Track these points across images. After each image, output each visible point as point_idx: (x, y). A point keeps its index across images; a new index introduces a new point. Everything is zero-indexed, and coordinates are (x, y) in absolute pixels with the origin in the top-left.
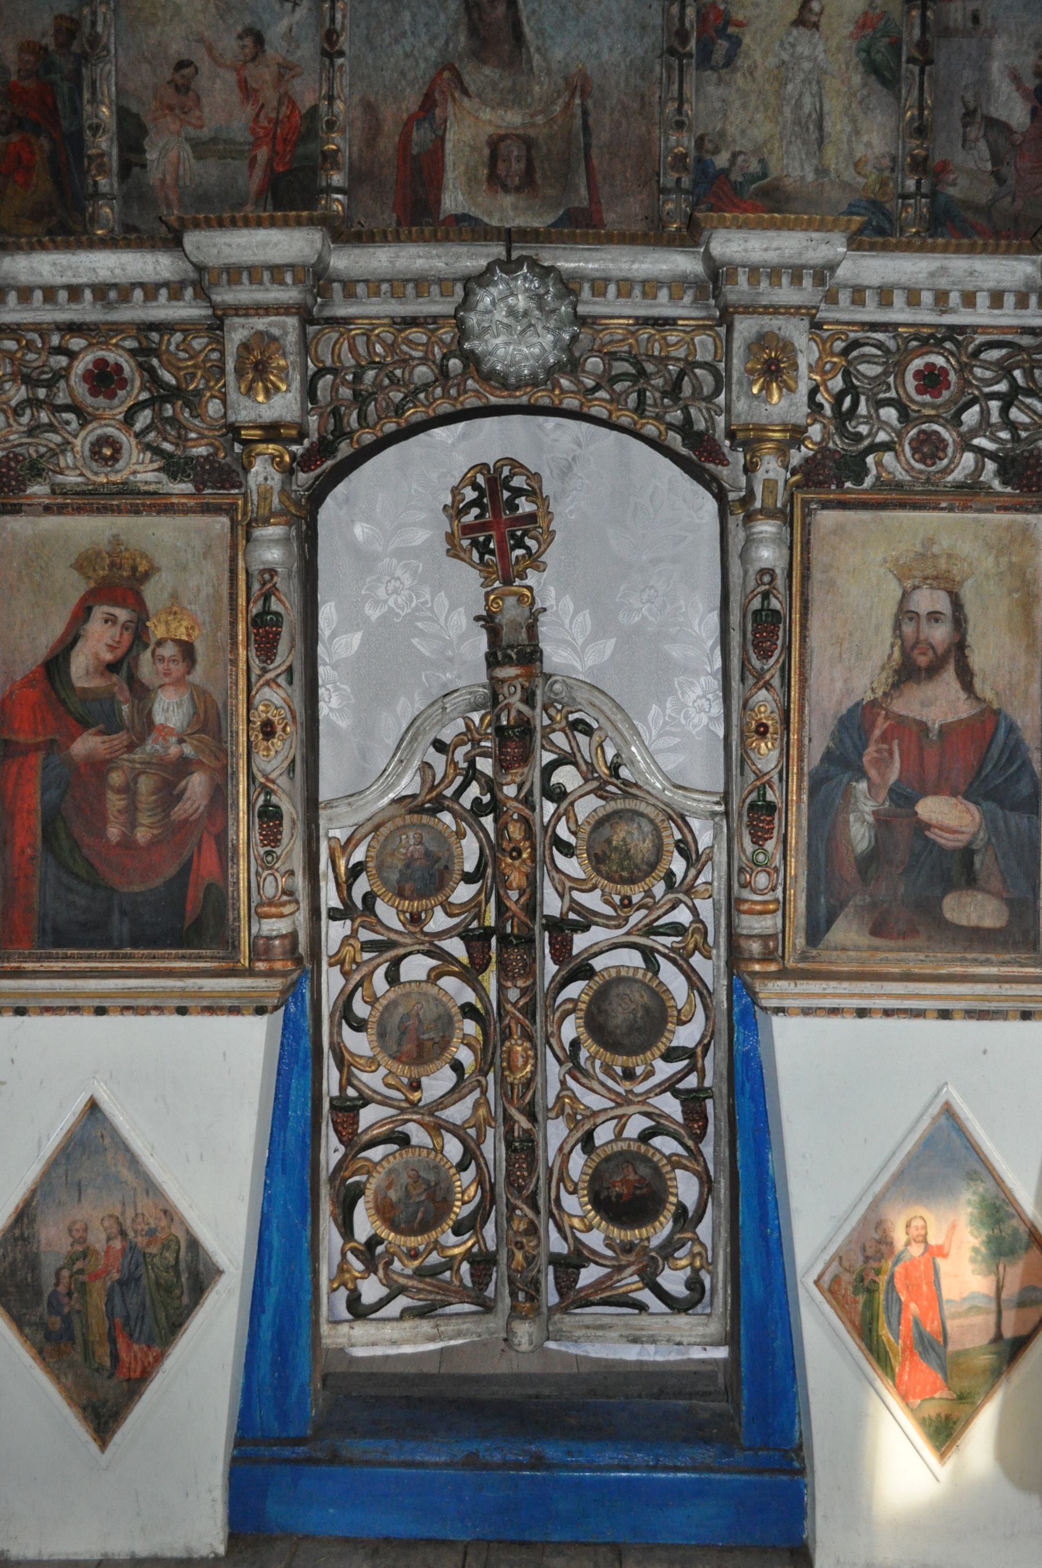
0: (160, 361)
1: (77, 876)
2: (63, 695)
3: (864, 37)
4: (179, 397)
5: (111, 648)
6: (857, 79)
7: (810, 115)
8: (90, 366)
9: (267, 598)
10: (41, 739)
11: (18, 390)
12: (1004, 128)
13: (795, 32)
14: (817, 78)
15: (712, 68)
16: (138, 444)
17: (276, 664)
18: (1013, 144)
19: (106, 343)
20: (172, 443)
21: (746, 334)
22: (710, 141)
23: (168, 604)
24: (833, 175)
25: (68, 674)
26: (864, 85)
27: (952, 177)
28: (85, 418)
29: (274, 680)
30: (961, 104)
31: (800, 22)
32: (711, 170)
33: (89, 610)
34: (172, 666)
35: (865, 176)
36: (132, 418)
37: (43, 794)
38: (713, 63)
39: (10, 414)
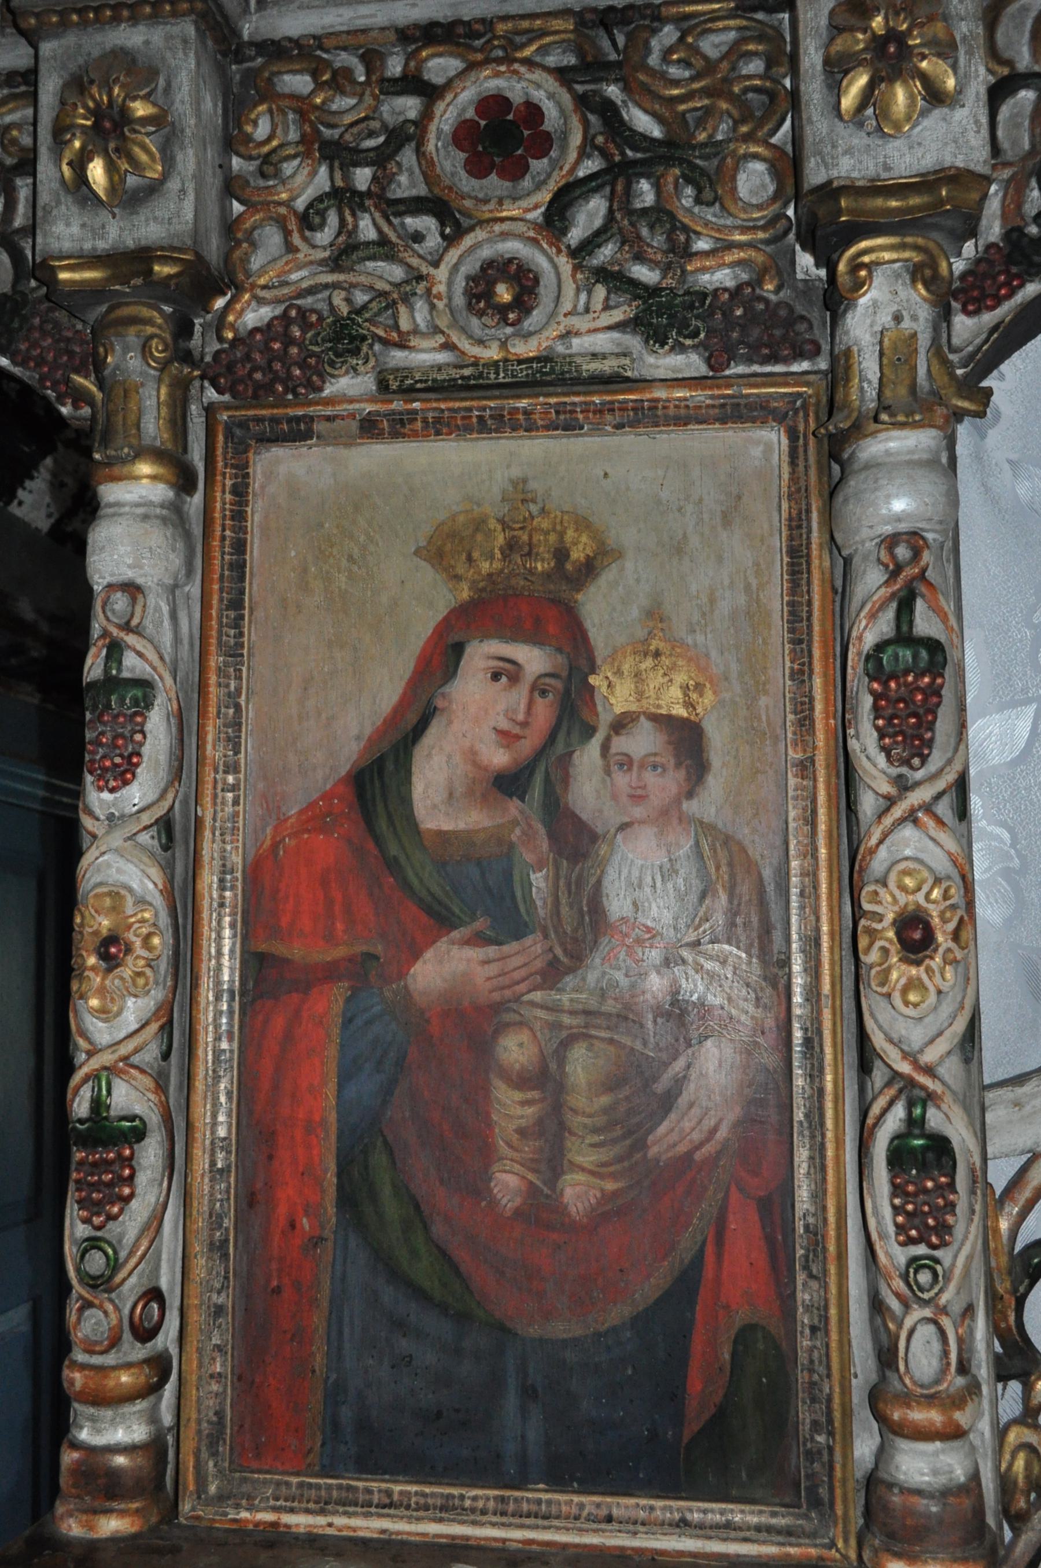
0: (626, 89)
1: (419, 1294)
2: (393, 850)
4: (668, 161)
5: (506, 737)
8: (470, 114)
9: (905, 606)
10: (340, 952)
11: (313, 173)
16: (577, 268)
17: (933, 765)
19: (509, 60)
20: (653, 264)
23: (641, 633)
25: (406, 801)
28: (457, 224)
29: (928, 808)
33: (458, 649)
34: (650, 778)
36: (563, 218)
37: (340, 1086)
39: (293, 225)
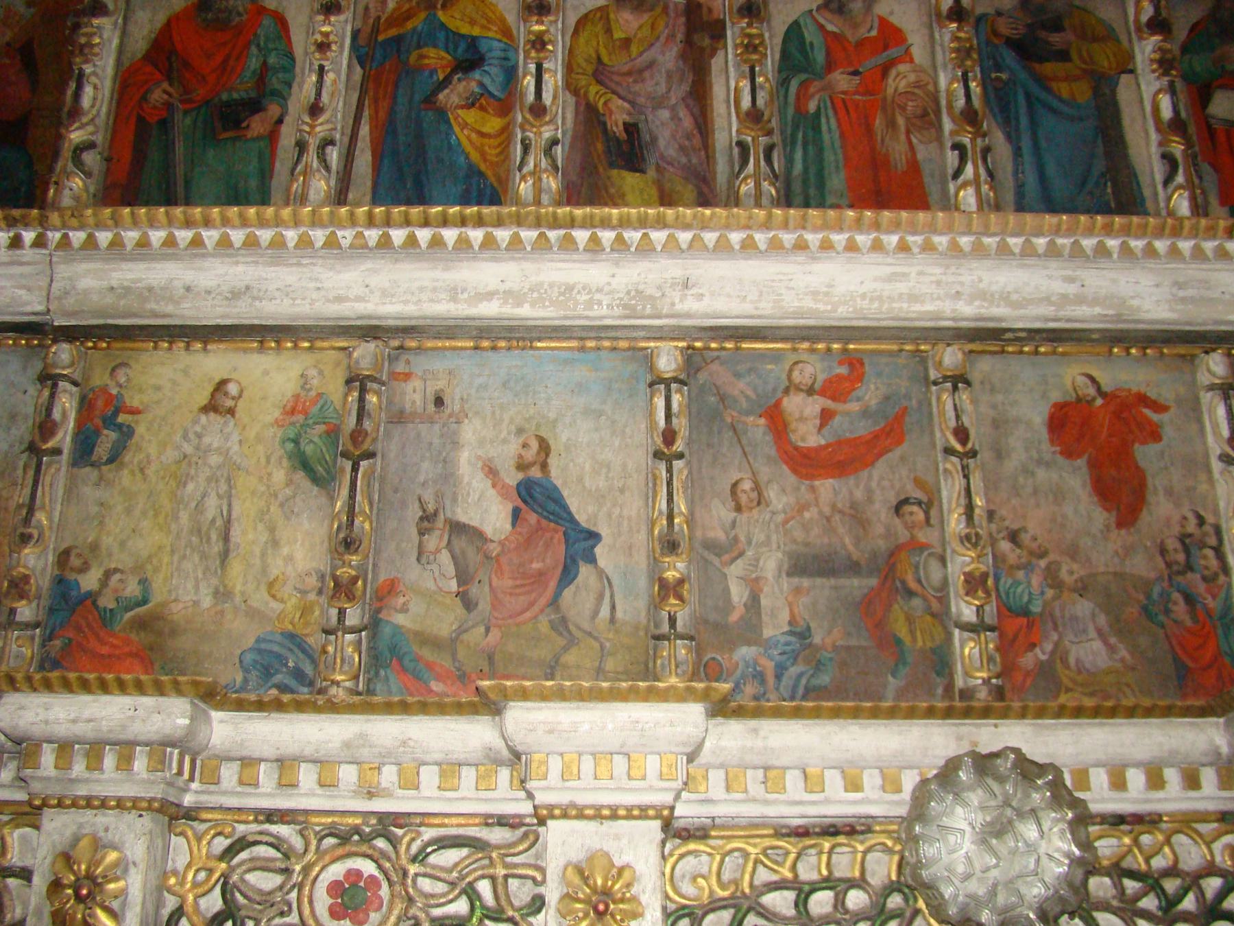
3: (293, 424)
6: (279, 476)
7: (213, 521)
12: (476, 535)
13: (203, 418)
14: (229, 474)
15: (92, 465)
18: (488, 557)
21: (56, 837)
22: (79, 555)
24: (238, 599)
26: (289, 483)
27: (401, 600)
30: (417, 504)
31: (211, 407)
32: (74, 593)
35: (282, 601)
38: (94, 458)
